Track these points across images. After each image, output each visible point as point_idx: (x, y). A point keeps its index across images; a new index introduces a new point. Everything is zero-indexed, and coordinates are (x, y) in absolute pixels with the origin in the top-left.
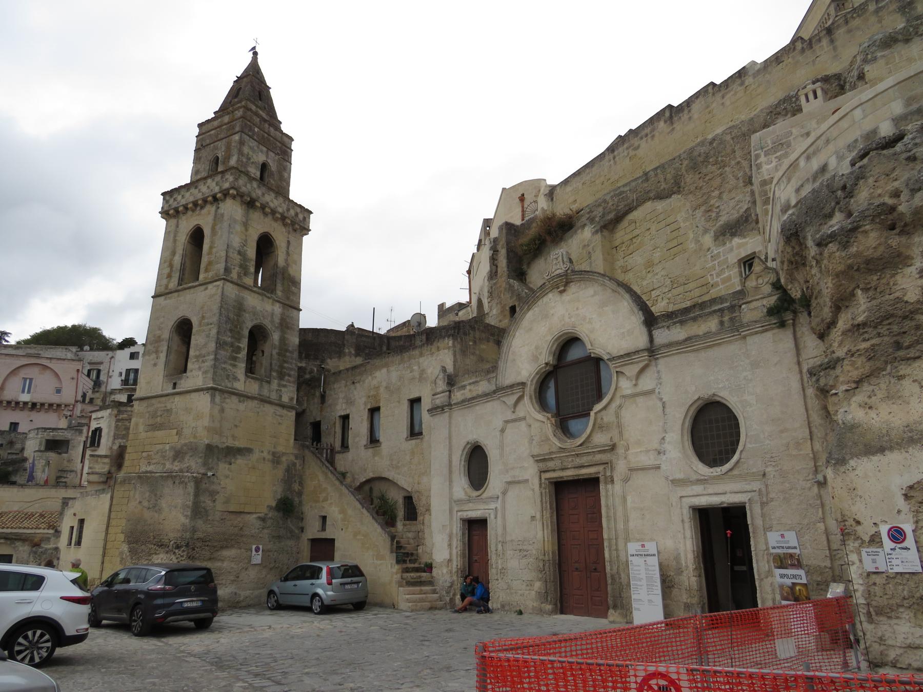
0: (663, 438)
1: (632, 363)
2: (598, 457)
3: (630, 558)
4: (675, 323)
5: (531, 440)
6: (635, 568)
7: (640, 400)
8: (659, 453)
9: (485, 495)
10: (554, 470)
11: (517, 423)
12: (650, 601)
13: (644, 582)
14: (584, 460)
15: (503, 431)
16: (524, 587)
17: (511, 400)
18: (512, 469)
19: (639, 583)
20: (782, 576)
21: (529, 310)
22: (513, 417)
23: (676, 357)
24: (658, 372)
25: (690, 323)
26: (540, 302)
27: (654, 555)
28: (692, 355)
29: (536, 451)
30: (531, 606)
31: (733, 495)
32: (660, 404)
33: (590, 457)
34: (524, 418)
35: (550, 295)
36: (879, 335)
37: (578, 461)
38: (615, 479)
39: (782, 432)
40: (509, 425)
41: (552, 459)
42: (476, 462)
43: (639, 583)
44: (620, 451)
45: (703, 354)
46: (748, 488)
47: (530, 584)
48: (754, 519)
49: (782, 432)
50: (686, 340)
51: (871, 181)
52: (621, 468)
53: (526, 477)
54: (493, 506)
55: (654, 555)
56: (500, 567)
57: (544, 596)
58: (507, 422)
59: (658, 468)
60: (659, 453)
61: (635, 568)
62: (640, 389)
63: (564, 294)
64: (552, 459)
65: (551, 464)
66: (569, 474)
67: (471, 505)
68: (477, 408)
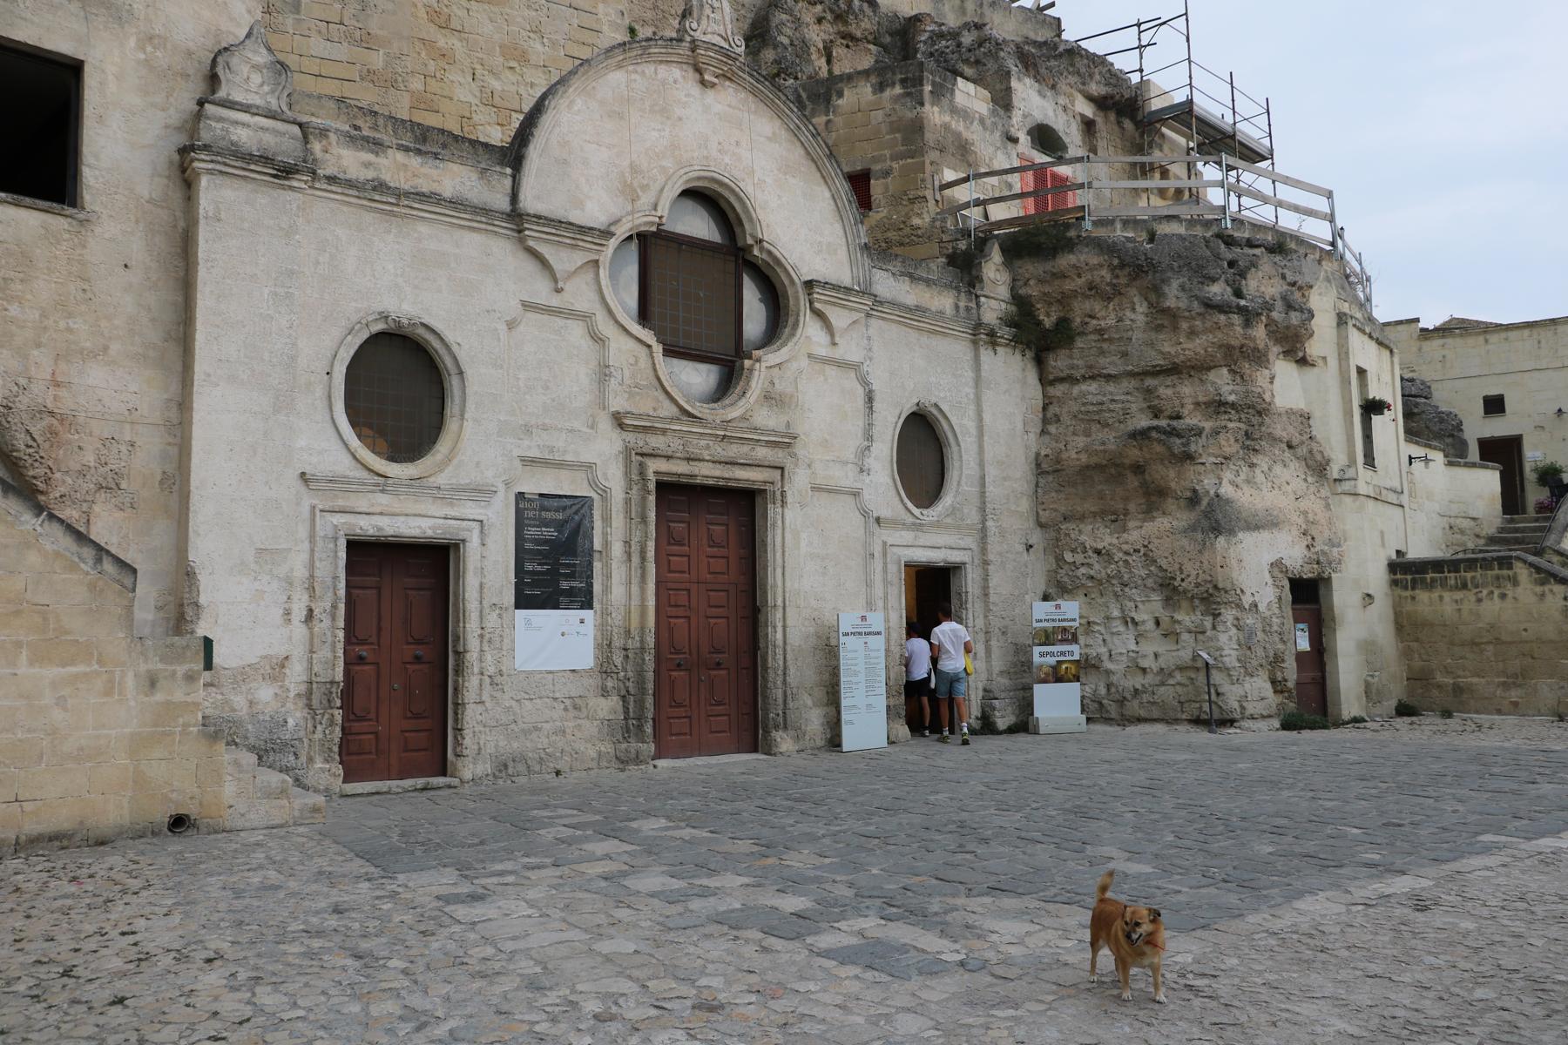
0: (868, 448)
1: (844, 307)
2: (762, 453)
3: (843, 639)
4: (902, 274)
5: (603, 373)
6: (850, 655)
7: (831, 371)
8: (862, 471)
9: (441, 480)
10: (668, 458)
11: (559, 322)
12: (869, 706)
13: (862, 677)
14: (733, 451)
15: (511, 325)
16: (558, 712)
17: (564, 259)
18: (545, 428)
19: (854, 679)
20: (1042, 655)
21: (619, 67)
22: (555, 301)
23: (894, 326)
24: (869, 338)
25: (922, 286)
26: (649, 69)
27: (879, 633)
28: (913, 334)
29: (618, 403)
30: (592, 753)
31: (949, 552)
32: (860, 391)
33: (745, 449)
34: (585, 317)
35: (676, 72)
36: (1240, 420)
37: (720, 451)
38: (789, 499)
39: (1005, 479)
40: (530, 315)
41: (664, 431)
42: (399, 386)
43: (854, 679)
44: (799, 450)
45: (924, 339)
46: (962, 544)
47: (576, 705)
48: (970, 582)
49: (1005, 479)
50: (918, 308)
51: (1260, 274)
52: (799, 482)
53: (586, 457)
54: (471, 510)
55: (879, 633)
56: (491, 670)
57: (630, 726)
58: (527, 306)
59: (856, 494)
60: (862, 471)
61: (850, 655)
62: (838, 353)
63: (710, 93)
64: (664, 431)
65: (656, 442)
66: (707, 473)
67: (383, 500)
68: (423, 229)
